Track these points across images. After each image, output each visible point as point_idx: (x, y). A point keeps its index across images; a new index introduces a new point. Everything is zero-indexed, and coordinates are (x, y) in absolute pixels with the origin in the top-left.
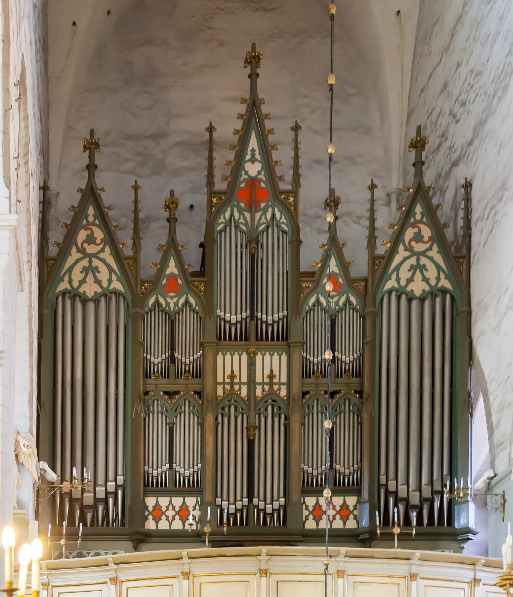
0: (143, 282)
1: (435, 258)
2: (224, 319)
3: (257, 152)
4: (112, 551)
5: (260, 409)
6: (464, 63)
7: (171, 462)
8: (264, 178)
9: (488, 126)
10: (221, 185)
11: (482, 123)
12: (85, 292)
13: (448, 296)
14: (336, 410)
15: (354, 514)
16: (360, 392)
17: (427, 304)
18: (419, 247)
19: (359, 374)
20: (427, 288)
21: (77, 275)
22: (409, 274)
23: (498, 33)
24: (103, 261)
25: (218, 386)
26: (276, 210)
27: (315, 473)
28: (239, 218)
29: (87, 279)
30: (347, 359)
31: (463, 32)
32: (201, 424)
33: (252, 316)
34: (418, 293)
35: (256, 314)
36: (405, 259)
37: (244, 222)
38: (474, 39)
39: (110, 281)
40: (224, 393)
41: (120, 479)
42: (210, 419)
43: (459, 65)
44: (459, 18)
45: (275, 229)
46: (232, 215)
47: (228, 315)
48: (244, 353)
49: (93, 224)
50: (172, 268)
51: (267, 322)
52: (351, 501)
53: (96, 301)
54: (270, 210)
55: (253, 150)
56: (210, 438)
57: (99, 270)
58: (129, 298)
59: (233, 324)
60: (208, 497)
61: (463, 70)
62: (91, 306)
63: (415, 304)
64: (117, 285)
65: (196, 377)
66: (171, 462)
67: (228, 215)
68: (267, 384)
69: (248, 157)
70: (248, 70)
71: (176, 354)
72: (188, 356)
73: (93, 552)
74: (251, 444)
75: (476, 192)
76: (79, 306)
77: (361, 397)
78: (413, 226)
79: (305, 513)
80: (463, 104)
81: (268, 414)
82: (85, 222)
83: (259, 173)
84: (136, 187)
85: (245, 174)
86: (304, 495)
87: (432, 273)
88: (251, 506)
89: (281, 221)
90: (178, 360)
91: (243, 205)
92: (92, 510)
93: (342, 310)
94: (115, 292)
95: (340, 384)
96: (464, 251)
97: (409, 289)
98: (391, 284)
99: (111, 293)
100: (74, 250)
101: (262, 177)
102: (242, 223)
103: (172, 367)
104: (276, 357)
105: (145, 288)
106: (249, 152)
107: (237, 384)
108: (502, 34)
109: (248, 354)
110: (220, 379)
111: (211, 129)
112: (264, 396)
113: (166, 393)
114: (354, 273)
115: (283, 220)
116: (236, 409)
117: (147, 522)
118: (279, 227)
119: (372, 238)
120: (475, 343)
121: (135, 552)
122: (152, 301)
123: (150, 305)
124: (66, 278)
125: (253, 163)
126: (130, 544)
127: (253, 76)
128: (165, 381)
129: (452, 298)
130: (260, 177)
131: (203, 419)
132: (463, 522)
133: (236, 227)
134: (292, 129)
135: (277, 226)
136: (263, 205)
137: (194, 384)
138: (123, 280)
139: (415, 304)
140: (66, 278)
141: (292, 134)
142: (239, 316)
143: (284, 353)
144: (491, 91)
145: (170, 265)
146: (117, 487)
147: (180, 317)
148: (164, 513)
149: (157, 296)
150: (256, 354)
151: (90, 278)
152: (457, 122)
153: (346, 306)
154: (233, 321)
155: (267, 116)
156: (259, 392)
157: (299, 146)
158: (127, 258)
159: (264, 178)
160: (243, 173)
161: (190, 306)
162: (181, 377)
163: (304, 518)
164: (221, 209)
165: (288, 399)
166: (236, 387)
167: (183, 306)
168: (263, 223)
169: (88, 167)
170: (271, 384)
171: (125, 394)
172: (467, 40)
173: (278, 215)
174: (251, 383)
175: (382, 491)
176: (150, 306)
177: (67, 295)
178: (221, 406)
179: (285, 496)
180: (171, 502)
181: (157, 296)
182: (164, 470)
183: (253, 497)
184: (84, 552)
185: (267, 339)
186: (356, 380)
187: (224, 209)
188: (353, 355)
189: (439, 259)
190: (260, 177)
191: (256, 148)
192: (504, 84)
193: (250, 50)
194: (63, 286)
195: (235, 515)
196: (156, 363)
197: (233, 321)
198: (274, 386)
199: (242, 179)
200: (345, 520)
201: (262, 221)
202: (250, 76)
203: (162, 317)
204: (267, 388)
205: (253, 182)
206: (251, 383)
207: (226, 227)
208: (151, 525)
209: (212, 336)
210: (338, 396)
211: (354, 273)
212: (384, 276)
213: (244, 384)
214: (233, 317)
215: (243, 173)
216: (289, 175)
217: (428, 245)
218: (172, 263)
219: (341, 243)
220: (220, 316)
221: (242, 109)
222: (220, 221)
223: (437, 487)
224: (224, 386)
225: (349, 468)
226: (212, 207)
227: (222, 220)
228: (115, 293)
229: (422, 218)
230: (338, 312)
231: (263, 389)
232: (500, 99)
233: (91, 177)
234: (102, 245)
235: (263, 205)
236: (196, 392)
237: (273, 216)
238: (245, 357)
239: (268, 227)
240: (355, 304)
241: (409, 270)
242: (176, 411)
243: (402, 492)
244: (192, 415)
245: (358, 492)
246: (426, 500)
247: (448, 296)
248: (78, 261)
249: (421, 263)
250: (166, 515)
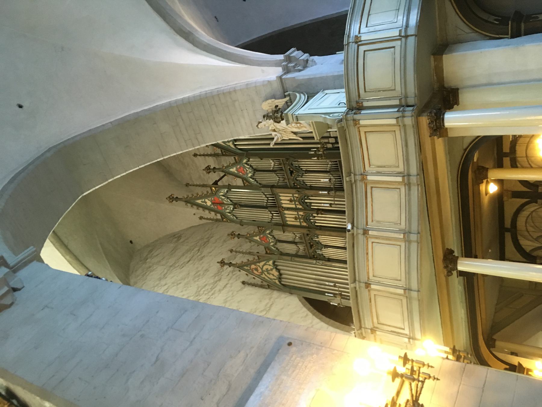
21: (271, 277)
24: (263, 266)
29: (272, 273)
39: (270, 265)
49: (250, 267)
50: (257, 238)
53: (279, 270)
55: (201, 202)
64: (271, 262)
67: (229, 214)
82: (250, 270)
100: (262, 276)
106: (203, 203)
115: (223, 191)
124: (274, 281)
136: (220, 200)
159: (210, 198)
174: (296, 209)
191: (201, 200)
194: (277, 281)
218: (255, 238)
231: (297, 204)
235: (220, 200)
240: (246, 160)
248: (266, 275)
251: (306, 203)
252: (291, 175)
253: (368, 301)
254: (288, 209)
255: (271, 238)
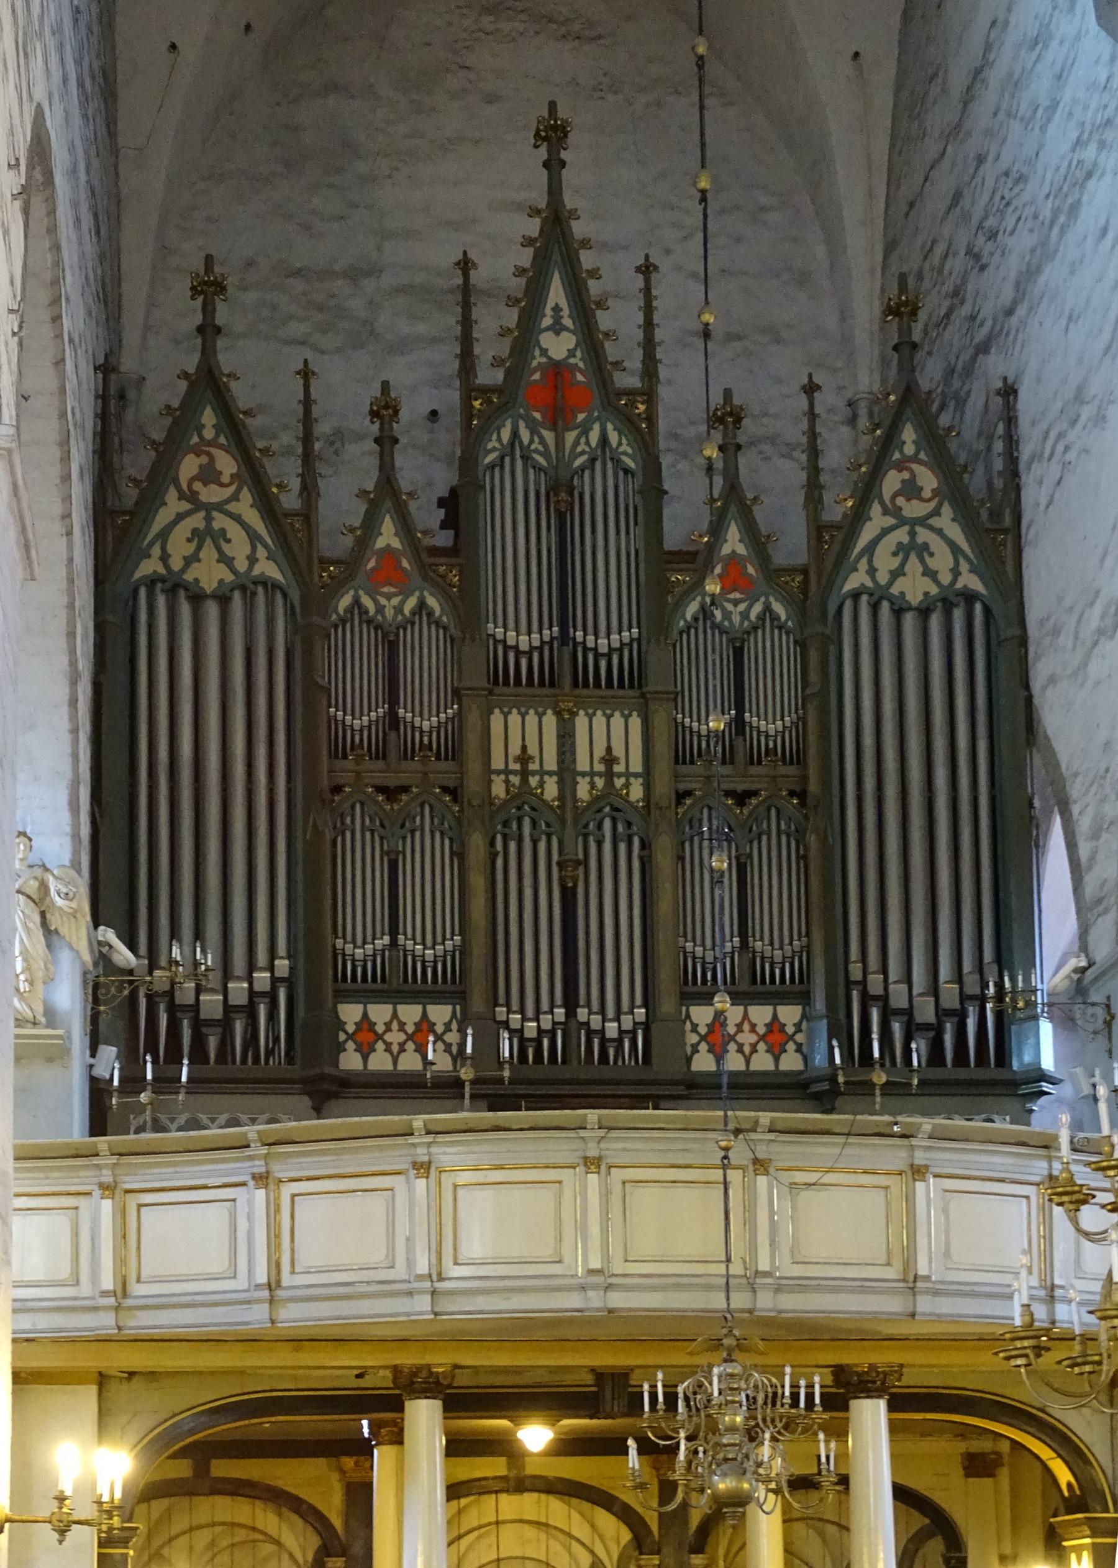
0: (325, 562)
1: (947, 532)
2: (504, 641)
3: (566, 312)
4: (267, 1116)
5: (586, 826)
6: (990, 158)
7: (394, 932)
8: (581, 365)
9: (1043, 279)
10: (489, 376)
11: (1031, 273)
12: (197, 580)
13: (978, 607)
14: (751, 830)
15: (796, 1043)
16: (802, 795)
17: (935, 621)
18: (913, 509)
19: (798, 758)
20: (934, 590)
22: (895, 563)
23: (1055, 104)
25: (493, 777)
26: (610, 427)
27: (709, 957)
28: (531, 441)
30: (771, 726)
31: (988, 98)
32: (459, 854)
33: (565, 638)
34: (915, 598)
35: (572, 635)
36: (885, 532)
37: (541, 448)
38: (1009, 114)
40: (508, 792)
41: (282, 965)
42: (477, 842)
43: (980, 160)
44: (978, 71)
45: (610, 465)
46: (515, 434)
47: (511, 634)
48: (549, 712)
50: (388, 536)
51: (595, 649)
52: (789, 1014)
54: (597, 427)
56: (478, 882)
57: (228, 536)
58: (295, 595)
59: (524, 652)
60: (478, 1004)
61: (989, 172)
62: (212, 610)
63: (909, 621)
65: (446, 759)
66: (394, 932)
67: (506, 434)
68: (600, 774)
69: (547, 321)
70: (543, 153)
71: (401, 711)
72: (426, 716)
73: (223, 1118)
74: (568, 897)
75: (1025, 403)
76: (185, 609)
77: (803, 804)
78: (900, 467)
79: (693, 1038)
80: (993, 235)
81: (603, 836)
83: (571, 353)
84: (306, 373)
85: (541, 355)
86: (686, 1002)
87: (942, 561)
88: (573, 1025)
89: (621, 449)
90: (405, 722)
91: (537, 415)
92: (219, 1030)
93: (755, 628)
94: (264, 582)
95: (757, 777)
96: (1008, 521)
97: (895, 590)
98: (856, 580)
99: (255, 583)
101: (577, 360)
102: (536, 451)
103: (392, 735)
104: (617, 721)
105: (329, 576)
106: (548, 312)
107: (534, 773)
108: (1061, 105)
109: (558, 713)
110: (498, 763)
111: (465, 265)
112: (595, 800)
113: (380, 789)
114: (780, 559)
115: (625, 447)
116: (534, 824)
117: (342, 1056)
118: (617, 462)
119: (814, 489)
120: (1036, 701)
121: (319, 1117)
122: (345, 601)
123: (341, 610)
125: (558, 333)
126: (306, 1102)
127: (554, 166)
128: (380, 764)
129: (987, 611)
130: (572, 361)
131: (462, 844)
132: (1027, 1058)
133: (526, 458)
134: (638, 269)
135: (612, 459)
136: (581, 417)
137: (443, 771)
138: (281, 559)
139: (909, 621)
140: (156, 551)
141: (640, 278)
142: (535, 636)
143: (635, 713)
144: (1046, 213)
145: (384, 529)
146: (275, 981)
147: (407, 637)
148: (380, 1037)
149: (356, 592)
150: (574, 714)
151: (209, 553)
152: (983, 268)
153: (764, 620)
154: (524, 647)
155: (585, 243)
156: (583, 791)
157: (655, 304)
158: (287, 515)
159: (581, 365)
160: (537, 353)
161: (430, 614)
162: (412, 759)
163: (689, 1050)
164: (491, 420)
165: (647, 806)
166: (533, 781)
167: (413, 613)
168: (583, 453)
169: (201, 330)
170: (609, 775)
171: (290, 791)
172: (995, 114)
173: (613, 437)
174: (566, 772)
175: (855, 994)
176: (341, 611)
177: (159, 585)
178: (501, 817)
179: (645, 1005)
180: (395, 1015)
181: (356, 592)
182: (379, 947)
183: (577, 1005)
184: (204, 1118)
185: (597, 684)
186: (792, 770)
187: (498, 422)
188: (782, 719)
189: (955, 532)
190: (572, 361)
191: (563, 303)
192: (1070, 200)
193: (546, 114)
195: (538, 1042)
196: (357, 727)
197: (524, 647)
198: (615, 779)
199: (535, 363)
200: (777, 1053)
201: (579, 449)
202: (546, 164)
203: (369, 636)
204: (600, 782)
205: (557, 371)
206: (566, 772)
207: (502, 458)
208: (351, 1061)
209: (476, 678)
210: (754, 801)
211: (780, 559)
212: (841, 564)
213: (550, 774)
214: (524, 638)
215: (537, 353)
216: (635, 362)
217: (932, 505)
219: (750, 496)
220: (494, 636)
221: (533, 227)
222: (490, 446)
223: (972, 988)
224: (507, 777)
225: (781, 948)
226: (470, 418)
227: (493, 444)
228: (264, 584)
229: (917, 453)
230: (749, 633)
231: (593, 785)
232: (1064, 229)
233: (208, 353)
234: (233, 488)
235: (581, 417)
236: (445, 789)
237: (604, 441)
238: (550, 720)
239: (593, 460)
240: (783, 618)
241: (895, 554)
242: (405, 826)
243: (899, 997)
244: (438, 835)
245: (804, 998)
246: (950, 1013)
247: (978, 607)
249: (920, 540)
250: (385, 1042)
251: (600, 827)
252: (728, 794)
253: (868, 1167)
254: (566, 737)
255: (403, 602)
